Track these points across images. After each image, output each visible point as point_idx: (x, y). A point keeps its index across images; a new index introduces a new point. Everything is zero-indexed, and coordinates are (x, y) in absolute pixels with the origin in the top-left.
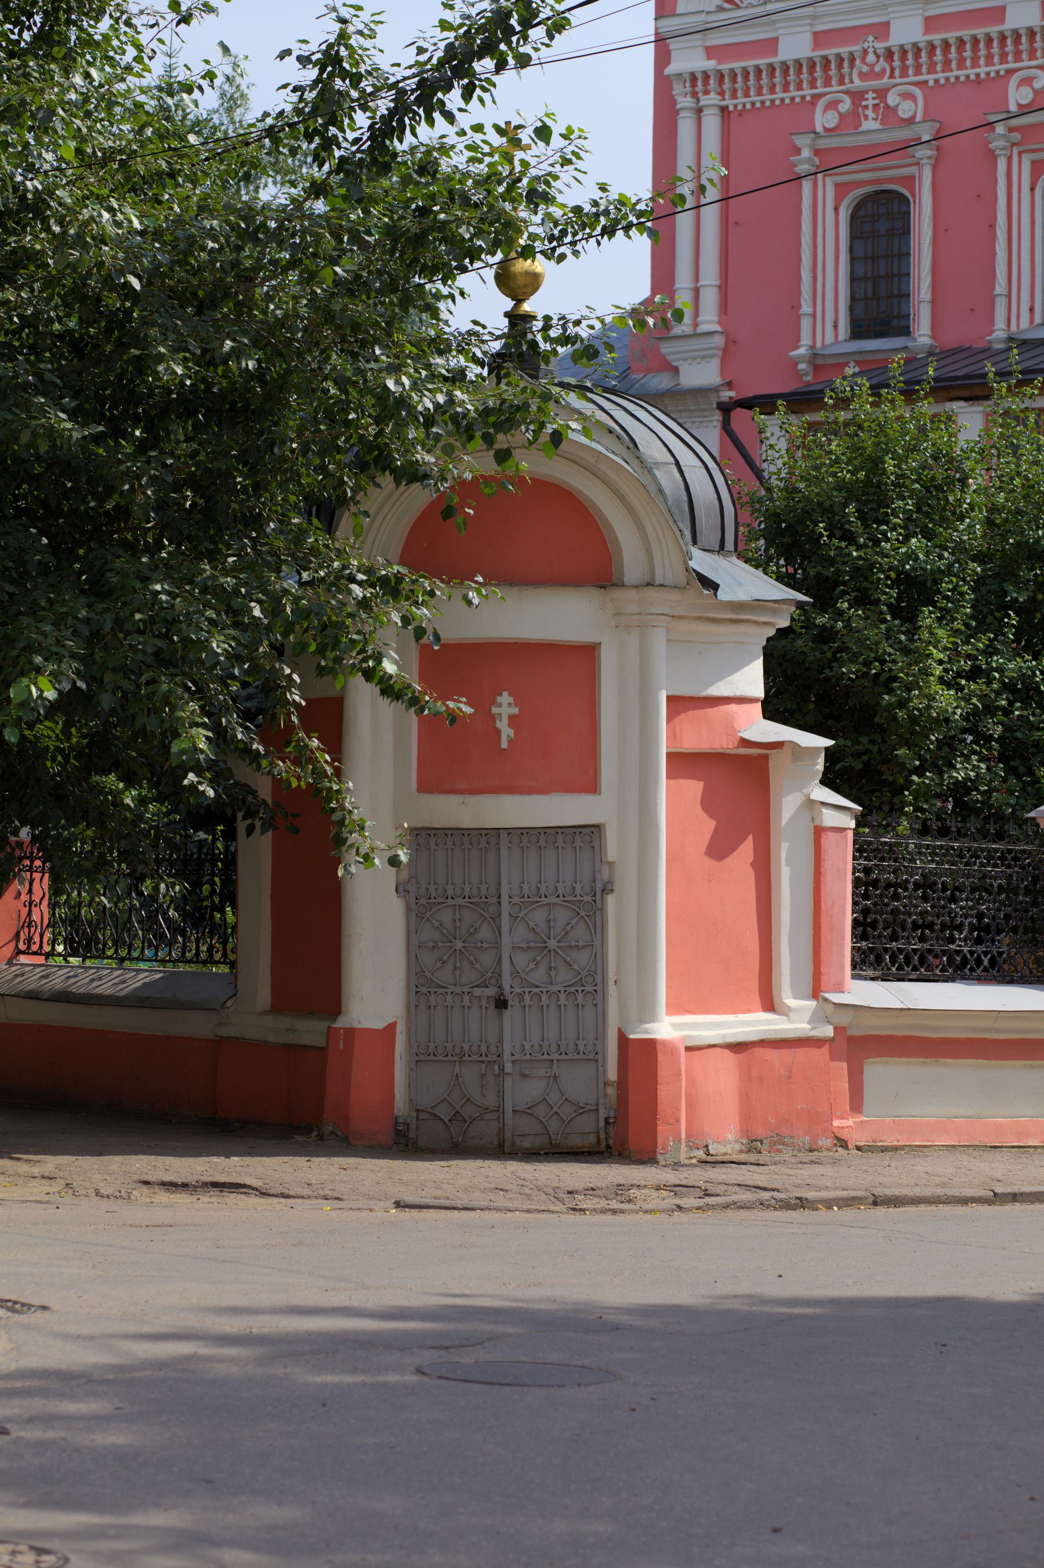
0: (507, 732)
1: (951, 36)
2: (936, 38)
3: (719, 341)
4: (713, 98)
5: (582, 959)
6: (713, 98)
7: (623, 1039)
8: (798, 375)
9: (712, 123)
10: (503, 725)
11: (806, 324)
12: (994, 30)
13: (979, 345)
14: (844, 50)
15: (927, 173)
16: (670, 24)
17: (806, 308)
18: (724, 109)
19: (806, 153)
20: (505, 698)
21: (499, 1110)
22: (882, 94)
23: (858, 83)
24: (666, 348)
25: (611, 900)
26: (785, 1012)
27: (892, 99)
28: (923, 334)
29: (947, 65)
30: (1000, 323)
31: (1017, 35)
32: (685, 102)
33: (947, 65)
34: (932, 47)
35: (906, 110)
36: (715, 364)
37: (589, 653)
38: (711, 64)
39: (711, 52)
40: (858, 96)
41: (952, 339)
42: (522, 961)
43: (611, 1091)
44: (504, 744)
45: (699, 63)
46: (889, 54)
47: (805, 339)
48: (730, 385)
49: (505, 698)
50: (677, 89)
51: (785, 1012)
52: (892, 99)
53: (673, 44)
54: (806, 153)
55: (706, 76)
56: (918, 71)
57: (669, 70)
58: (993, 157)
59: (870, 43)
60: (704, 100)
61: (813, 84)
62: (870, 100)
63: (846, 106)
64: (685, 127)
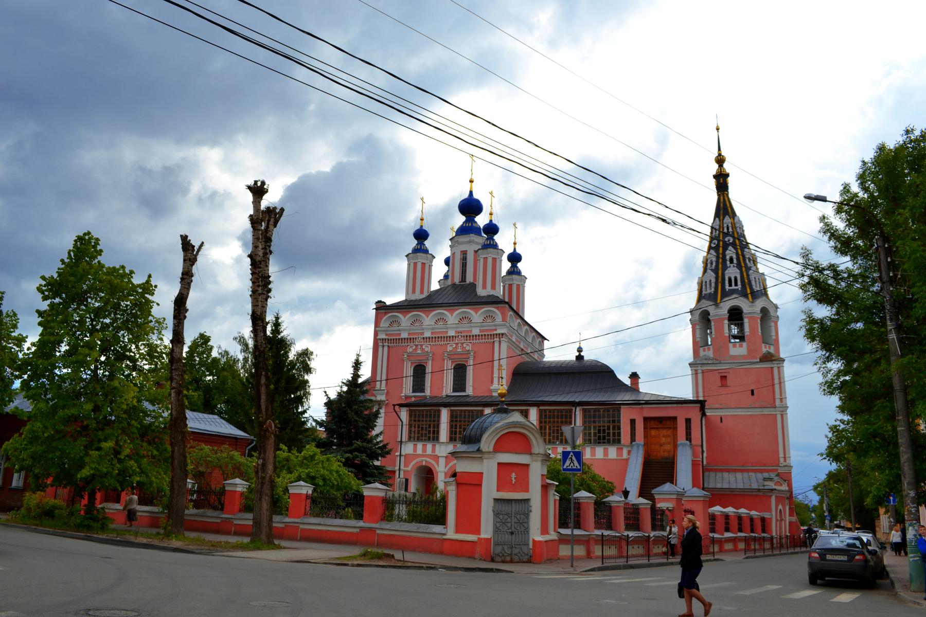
0: (514, 481)
1: (437, 336)
2: (433, 336)
3: (386, 391)
4: (386, 344)
5: (526, 525)
6: (386, 344)
7: (534, 540)
8: (402, 399)
9: (386, 349)
10: (513, 479)
11: (404, 389)
12: (445, 335)
13: (440, 396)
14: (414, 337)
15: (430, 362)
16: (377, 329)
17: (404, 386)
18: (388, 346)
19: (405, 356)
20: (514, 474)
21: (511, 554)
22: (421, 346)
23: (417, 343)
24: (374, 392)
25: (531, 514)
26: (551, 534)
27: (424, 347)
28: (428, 392)
29: (435, 341)
30: (444, 392)
31: (450, 337)
32: (381, 344)
33: (435, 341)
34: (432, 338)
35: (426, 349)
36: (385, 396)
37: (527, 466)
38: (386, 337)
39: (386, 335)
40: (417, 346)
41: (434, 395)
42: (516, 525)
43: (531, 551)
44: (513, 483)
45: (384, 336)
46: (424, 338)
47: (404, 392)
48: (387, 400)
49: (514, 474)
50: (379, 341)
51: (551, 534)
52: (424, 347)
53: (379, 333)
54: (405, 356)
55: (385, 339)
56: (429, 342)
57: (378, 337)
58: (444, 360)
59: (420, 336)
60: (385, 344)
61: (407, 343)
62: (419, 347)
63: (414, 347)
64: (380, 349)
